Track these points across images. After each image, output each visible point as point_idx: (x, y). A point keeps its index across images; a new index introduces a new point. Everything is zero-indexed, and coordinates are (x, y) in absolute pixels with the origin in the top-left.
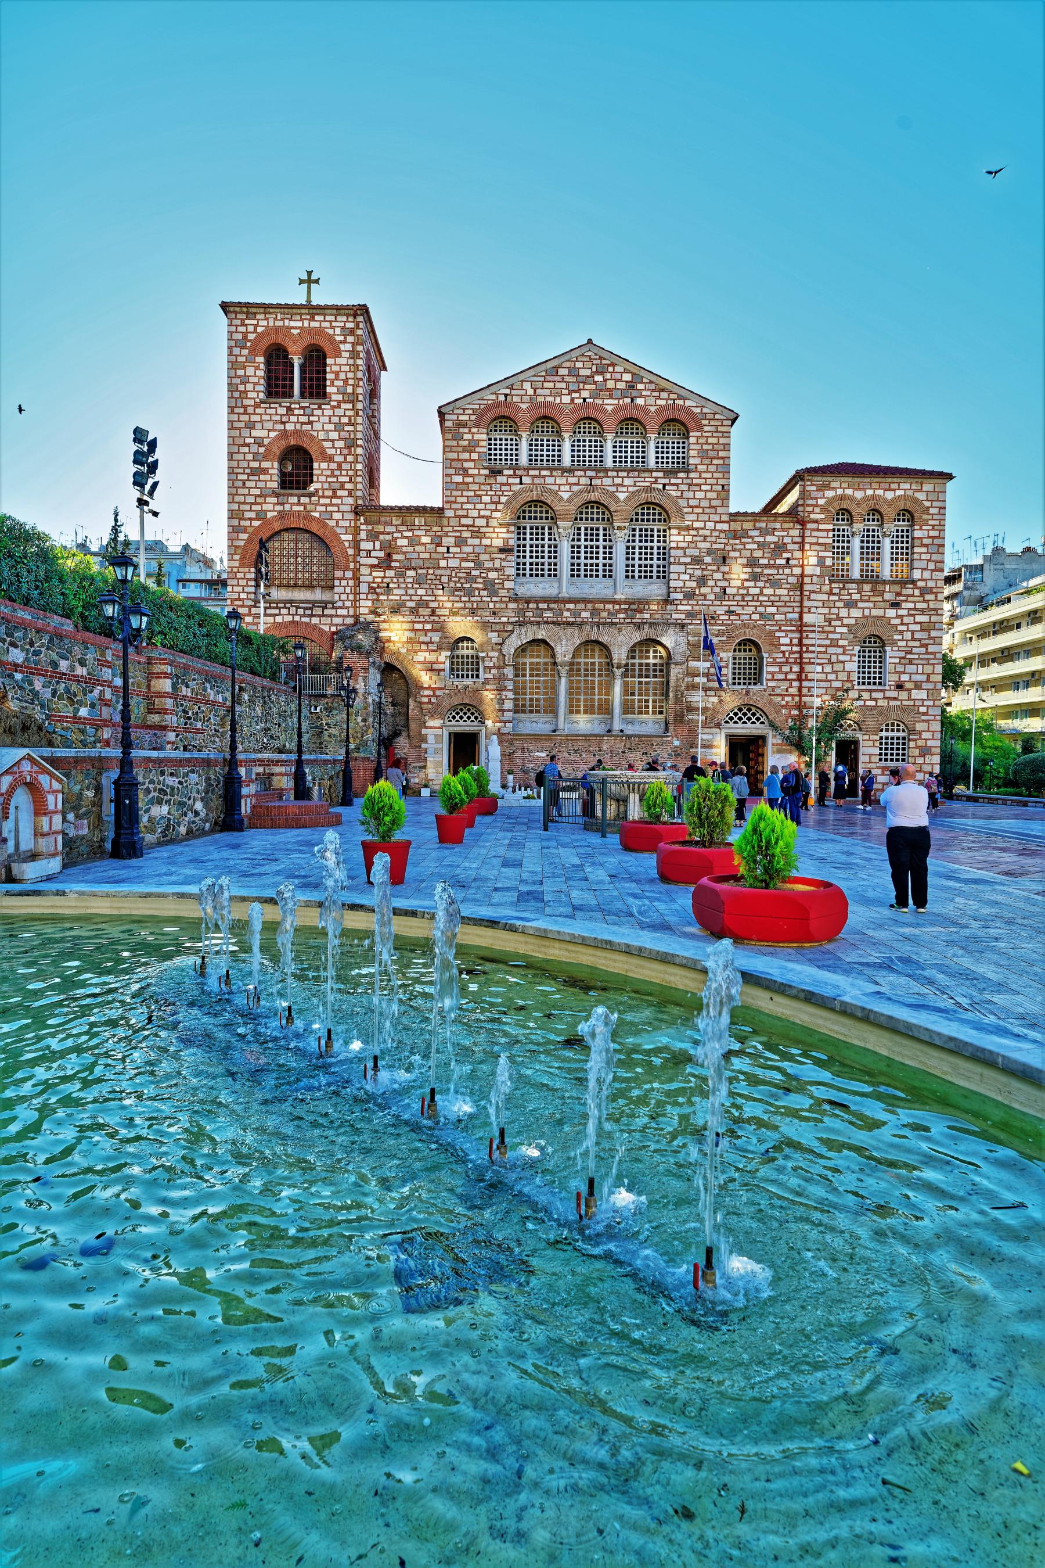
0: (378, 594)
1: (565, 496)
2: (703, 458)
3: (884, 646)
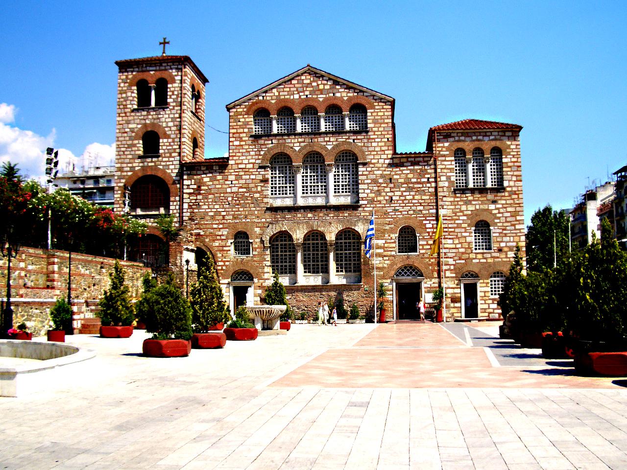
0: (193, 209)
1: (297, 149)
2: (375, 123)
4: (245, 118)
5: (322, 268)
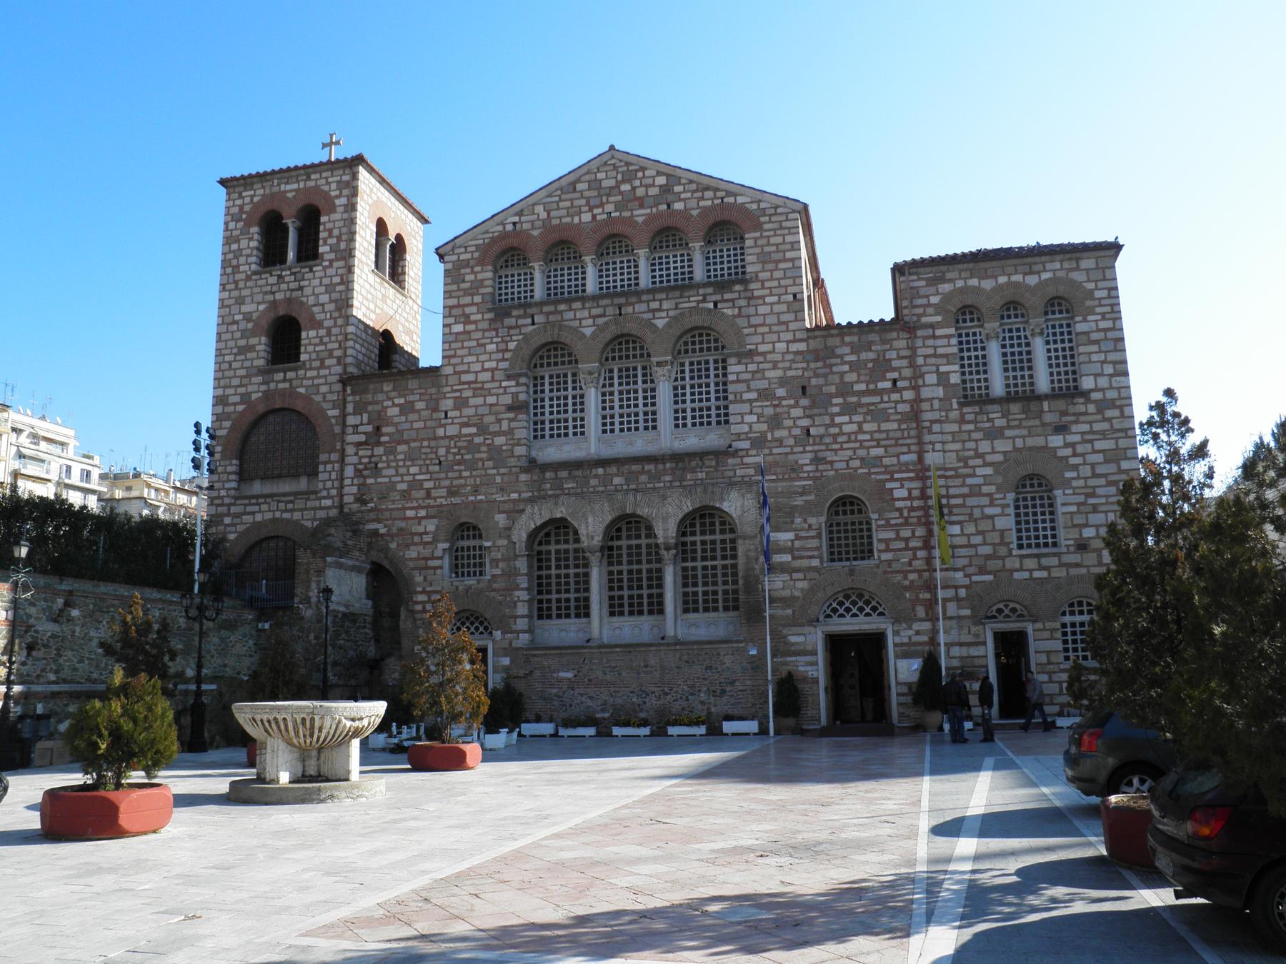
0: (365, 477)
1: (588, 332)
2: (764, 263)
3: (1051, 491)
4: (476, 273)
5: (650, 604)
